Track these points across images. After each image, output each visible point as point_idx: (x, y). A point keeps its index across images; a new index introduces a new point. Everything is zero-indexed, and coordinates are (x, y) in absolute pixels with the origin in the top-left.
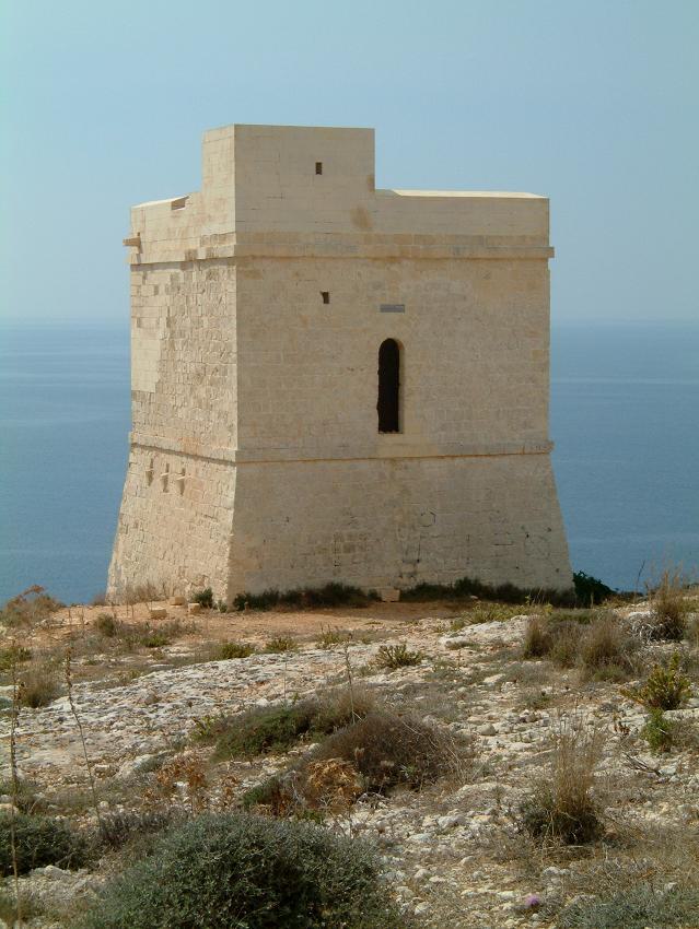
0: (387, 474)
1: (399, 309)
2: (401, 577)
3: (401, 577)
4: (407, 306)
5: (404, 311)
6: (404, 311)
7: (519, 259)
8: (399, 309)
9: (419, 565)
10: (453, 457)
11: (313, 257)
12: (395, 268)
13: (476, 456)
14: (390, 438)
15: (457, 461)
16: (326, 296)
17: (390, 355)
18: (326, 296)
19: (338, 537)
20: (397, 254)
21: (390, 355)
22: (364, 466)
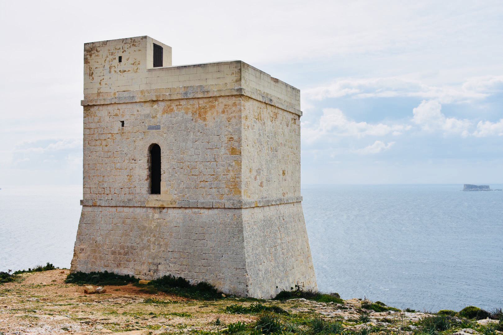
0: (151, 216)
1: (157, 128)
2: (149, 271)
3: (149, 271)
4: (162, 126)
5: (159, 129)
6: (159, 129)
7: (223, 96)
8: (157, 128)
9: (159, 266)
10: (186, 208)
11: (115, 103)
12: (155, 106)
13: (199, 208)
14: (155, 196)
15: (187, 211)
16: (123, 122)
17: (155, 152)
18: (123, 122)
19: (122, 248)
20: (154, 99)
21: (155, 152)
22: (138, 210)
